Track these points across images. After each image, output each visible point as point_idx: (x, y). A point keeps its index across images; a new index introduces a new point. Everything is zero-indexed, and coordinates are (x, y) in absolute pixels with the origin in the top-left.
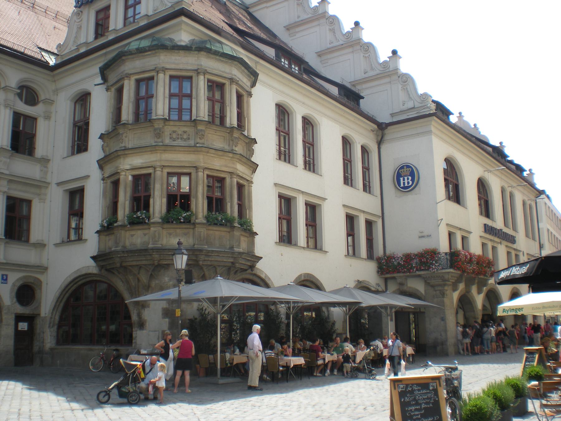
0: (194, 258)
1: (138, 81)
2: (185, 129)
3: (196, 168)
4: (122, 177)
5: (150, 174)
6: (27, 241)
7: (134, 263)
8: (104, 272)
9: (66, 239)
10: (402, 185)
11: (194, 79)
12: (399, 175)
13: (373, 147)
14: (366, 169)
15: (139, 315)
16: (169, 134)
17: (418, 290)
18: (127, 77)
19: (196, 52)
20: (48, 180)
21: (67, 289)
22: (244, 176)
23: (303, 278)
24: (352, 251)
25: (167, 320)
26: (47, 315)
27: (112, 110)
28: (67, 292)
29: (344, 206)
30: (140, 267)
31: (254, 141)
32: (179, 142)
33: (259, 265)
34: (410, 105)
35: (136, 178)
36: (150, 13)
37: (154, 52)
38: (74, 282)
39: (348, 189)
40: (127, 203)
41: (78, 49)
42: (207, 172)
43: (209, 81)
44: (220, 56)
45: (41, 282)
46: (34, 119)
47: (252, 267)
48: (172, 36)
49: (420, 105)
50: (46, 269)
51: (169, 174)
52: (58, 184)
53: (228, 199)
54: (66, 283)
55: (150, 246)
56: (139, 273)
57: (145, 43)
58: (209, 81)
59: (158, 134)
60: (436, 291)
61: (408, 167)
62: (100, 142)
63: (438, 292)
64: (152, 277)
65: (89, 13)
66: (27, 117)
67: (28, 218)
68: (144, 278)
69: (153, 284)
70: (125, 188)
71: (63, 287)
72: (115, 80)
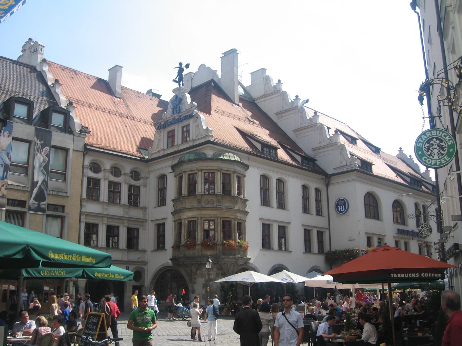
1: (189, 175)
2: (212, 198)
3: (217, 217)
4: (183, 222)
5: (196, 221)
6: (137, 249)
9: (156, 249)
10: (339, 211)
11: (216, 173)
12: (337, 205)
13: (322, 187)
14: (318, 201)
15: (192, 286)
20: (147, 218)
22: (241, 219)
23: (276, 267)
24: (308, 249)
29: (303, 225)
30: (192, 264)
31: (247, 200)
32: (209, 205)
33: (251, 261)
34: (344, 163)
35: (189, 222)
36: (194, 138)
39: (306, 215)
40: (186, 234)
41: (159, 152)
43: (223, 173)
45: (144, 269)
46: (138, 187)
47: (246, 263)
48: (205, 152)
50: (147, 263)
51: (204, 220)
52: (152, 221)
53: (233, 231)
54: (157, 270)
57: (192, 157)
58: (223, 173)
59: (199, 202)
61: (342, 200)
62: (172, 203)
64: (197, 269)
65: (164, 133)
66: (135, 186)
67: (137, 238)
68: (194, 269)
69: (198, 272)
70: (184, 227)
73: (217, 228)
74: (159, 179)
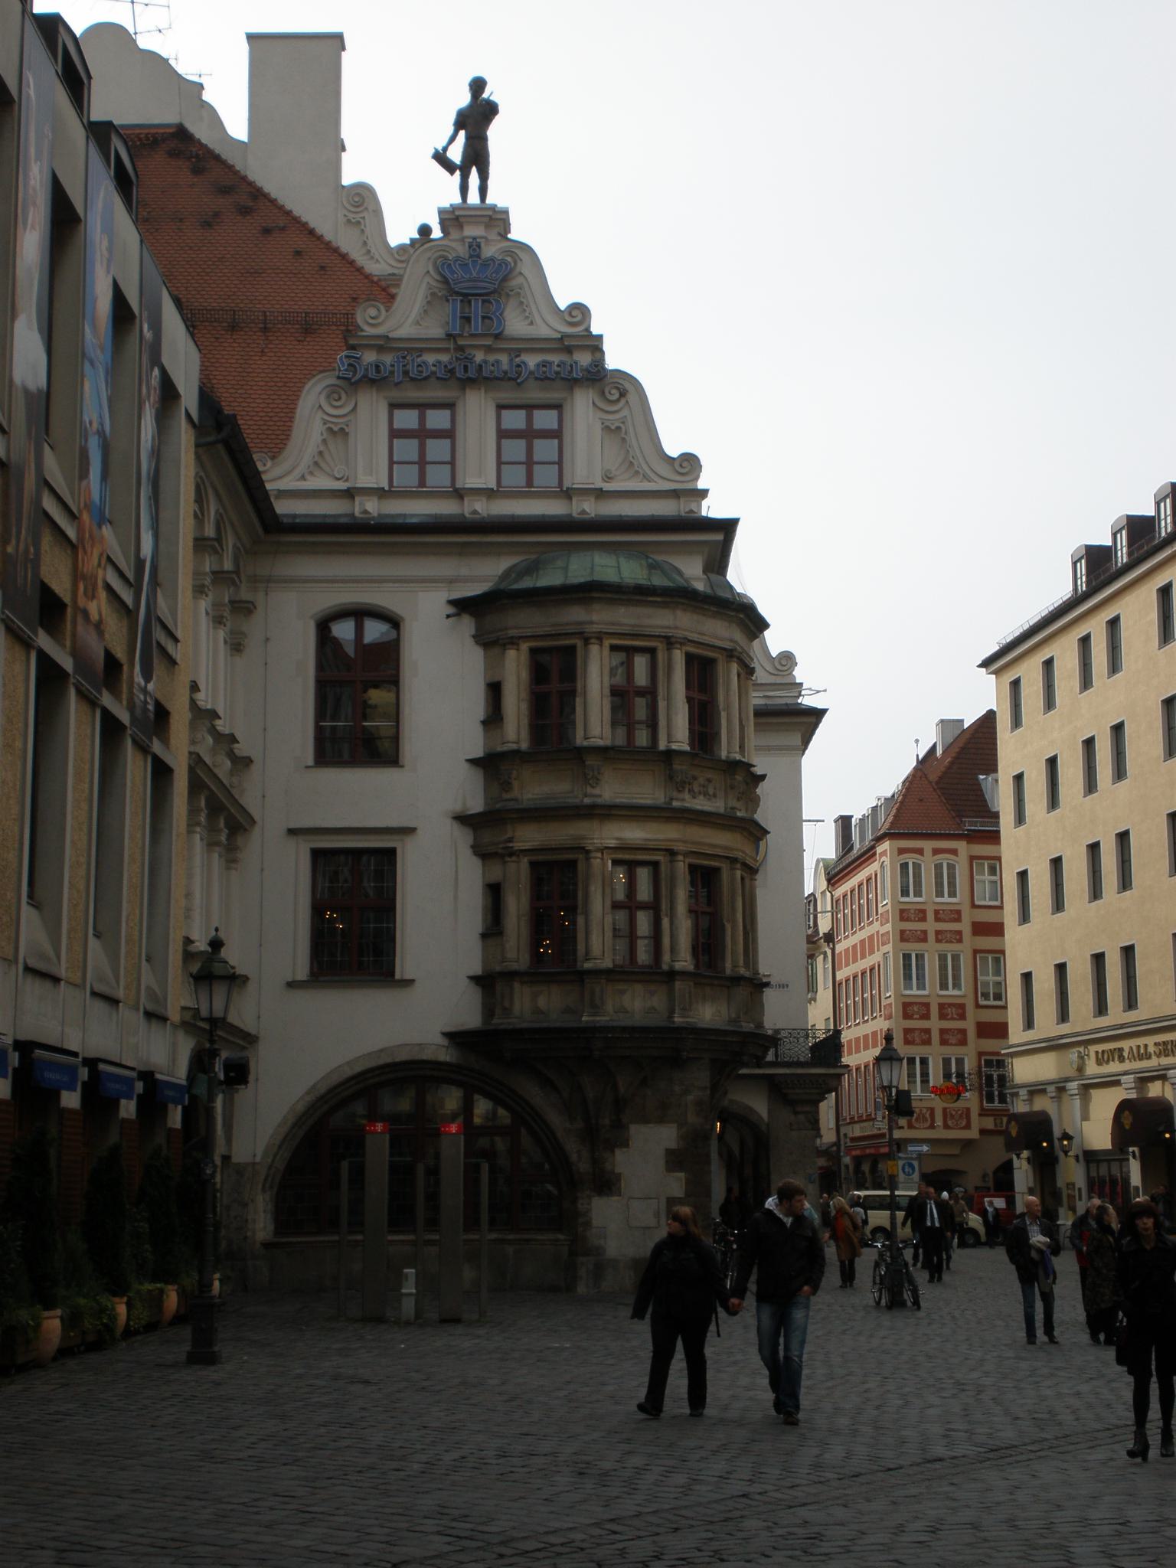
17: (751, 1110)
25: (682, 1175)
26: (258, 1159)
42: (689, 860)
49: (771, 680)
60: (796, 1113)
63: (801, 1117)
72: (548, 630)
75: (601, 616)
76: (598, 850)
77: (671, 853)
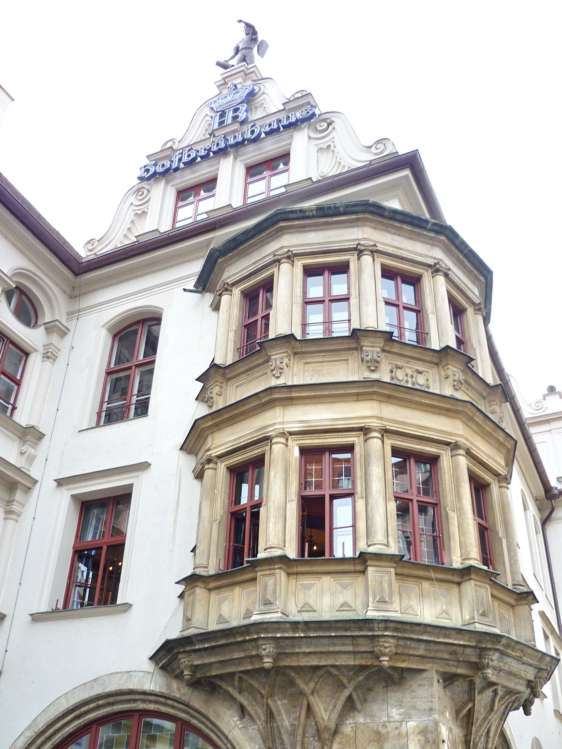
0: (474, 659)
7: (314, 661)
8: (178, 690)
16: (389, 368)
18: (289, 258)
19: (432, 235)
20: (34, 474)
21: (51, 731)
27: (234, 328)
28: (49, 738)
37: (354, 217)
38: (77, 713)
44: (465, 256)
55: (371, 614)
56: (312, 693)
64: (350, 706)
69: (347, 729)
70: (286, 472)
71: (42, 724)
73: (459, 497)
74: (114, 337)
75: (291, 241)
76: (282, 434)
77: (365, 431)
